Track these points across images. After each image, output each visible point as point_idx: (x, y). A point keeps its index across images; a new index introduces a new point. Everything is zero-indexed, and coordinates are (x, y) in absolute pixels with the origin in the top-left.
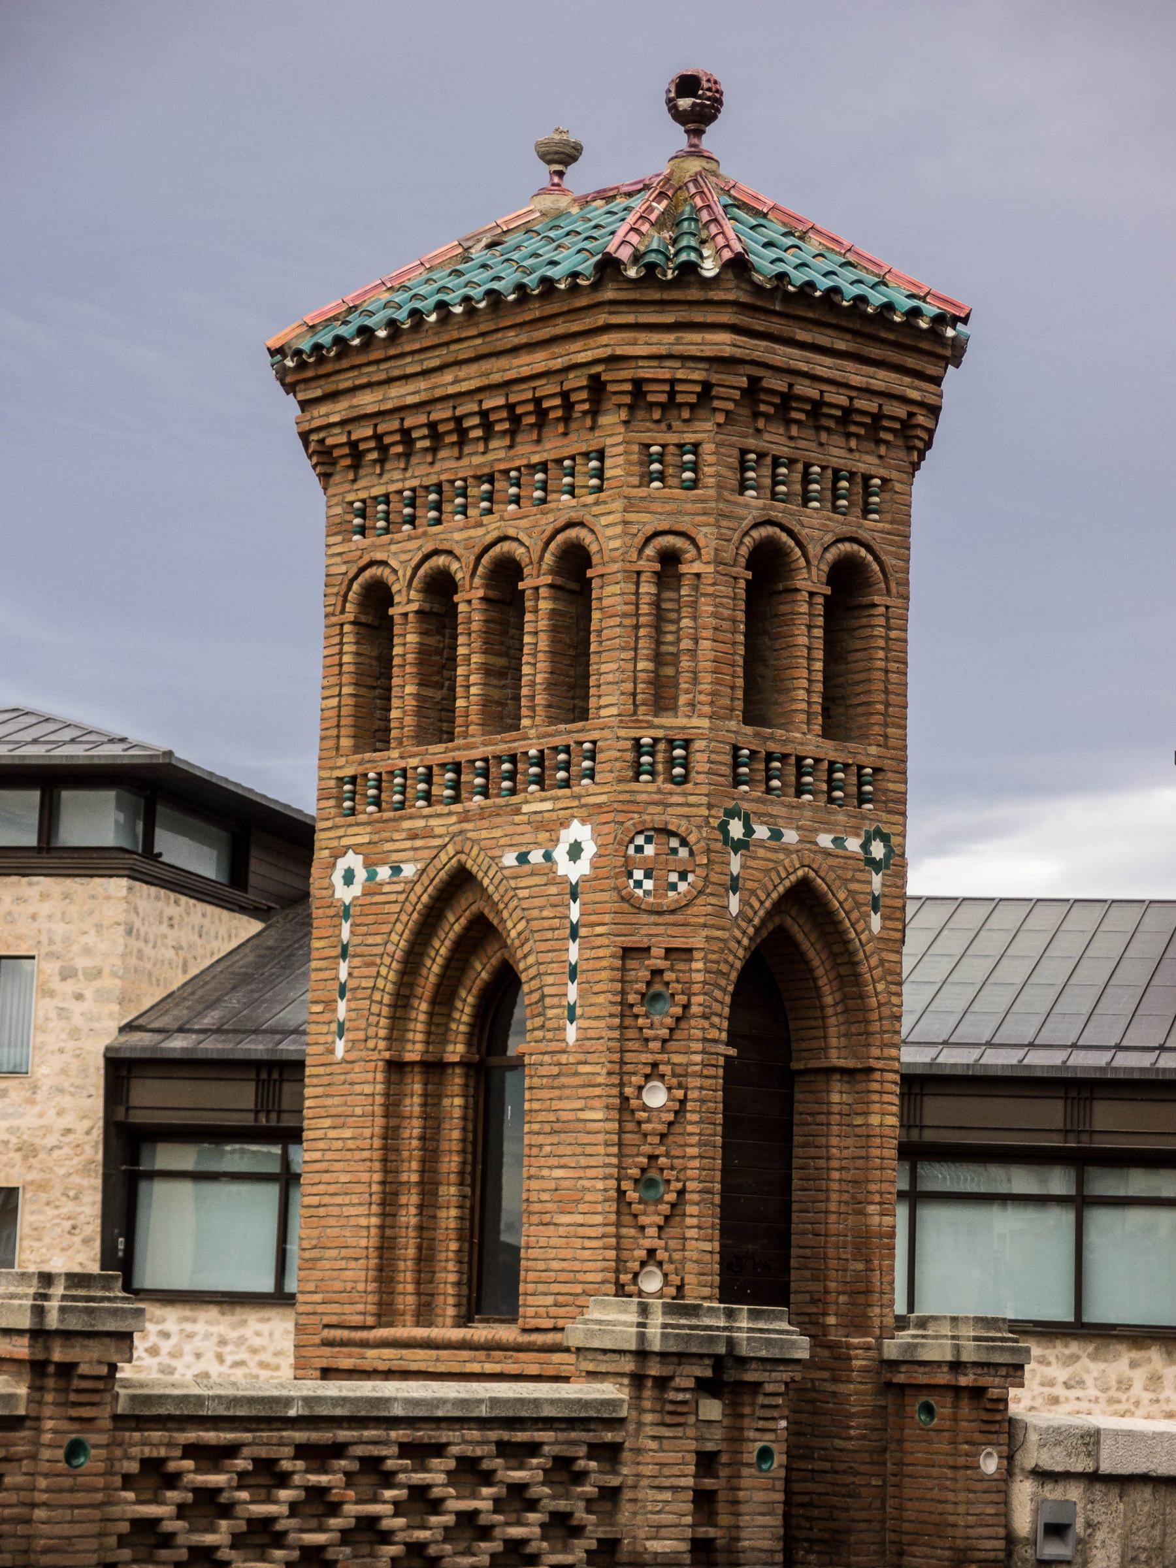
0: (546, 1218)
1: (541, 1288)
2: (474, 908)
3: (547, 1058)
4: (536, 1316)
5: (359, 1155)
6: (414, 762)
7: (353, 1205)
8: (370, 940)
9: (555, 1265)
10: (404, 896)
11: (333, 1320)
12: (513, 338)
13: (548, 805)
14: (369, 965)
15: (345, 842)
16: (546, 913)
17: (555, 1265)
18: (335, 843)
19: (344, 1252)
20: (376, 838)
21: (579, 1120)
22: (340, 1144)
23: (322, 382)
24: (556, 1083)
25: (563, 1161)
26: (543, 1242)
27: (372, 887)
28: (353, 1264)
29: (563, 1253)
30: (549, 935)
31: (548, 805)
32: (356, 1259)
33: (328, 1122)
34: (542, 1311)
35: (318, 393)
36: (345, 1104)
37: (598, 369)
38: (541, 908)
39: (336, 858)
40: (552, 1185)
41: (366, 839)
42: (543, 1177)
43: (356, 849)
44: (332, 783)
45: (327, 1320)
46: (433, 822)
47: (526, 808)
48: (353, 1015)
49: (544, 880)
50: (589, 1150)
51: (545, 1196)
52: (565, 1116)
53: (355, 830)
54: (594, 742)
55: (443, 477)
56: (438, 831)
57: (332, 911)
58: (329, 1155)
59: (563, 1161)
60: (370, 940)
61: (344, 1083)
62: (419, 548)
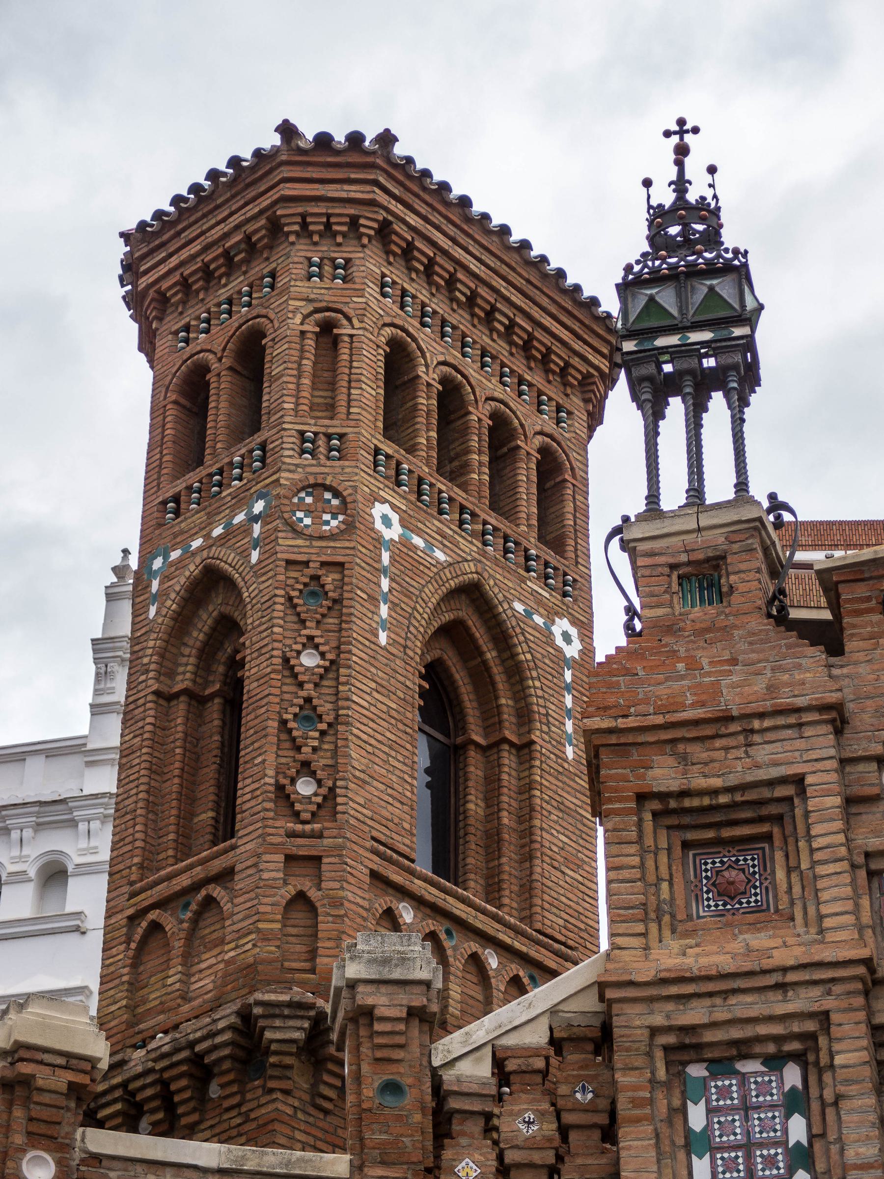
0: (556, 864)
1: (554, 910)
2: (461, 614)
3: (552, 756)
4: (551, 927)
5: (400, 726)
6: (444, 488)
7: (399, 761)
8: (407, 579)
9: (563, 899)
10: (435, 570)
11: (383, 838)
12: (545, 302)
13: (547, 595)
14: (406, 596)
15: (382, 493)
16: (547, 661)
17: (563, 899)
18: (376, 490)
19: (390, 791)
20: (411, 513)
21: (576, 811)
22: (385, 708)
23: (402, 189)
24: (560, 777)
25: (567, 832)
26: (553, 878)
27: (404, 542)
28: (398, 805)
29: (570, 896)
30: (550, 677)
31: (547, 595)
32: (402, 803)
33: (373, 685)
34: (557, 927)
35: (396, 192)
36: (388, 681)
37: (596, 373)
38: (544, 656)
39: (376, 500)
40: (561, 845)
41: (404, 508)
42: (552, 834)
43: (394, 507)
44: (373, 446)
45: (375, 834)
46: (456, 536)
47: (529, 583)
48: (394, 622)
49: (544, 639)
50: (584, 836)
51: (555, 849)
52: (567, 803)
53: (391, 492)
54: (575, 580)
55: (461, 326)
56: (462, 547)
57: (373, 535)
58: (373, 709)
59: (567, 832)
60: (407, 579)
61: (386, 665)
62: (442, 353)
